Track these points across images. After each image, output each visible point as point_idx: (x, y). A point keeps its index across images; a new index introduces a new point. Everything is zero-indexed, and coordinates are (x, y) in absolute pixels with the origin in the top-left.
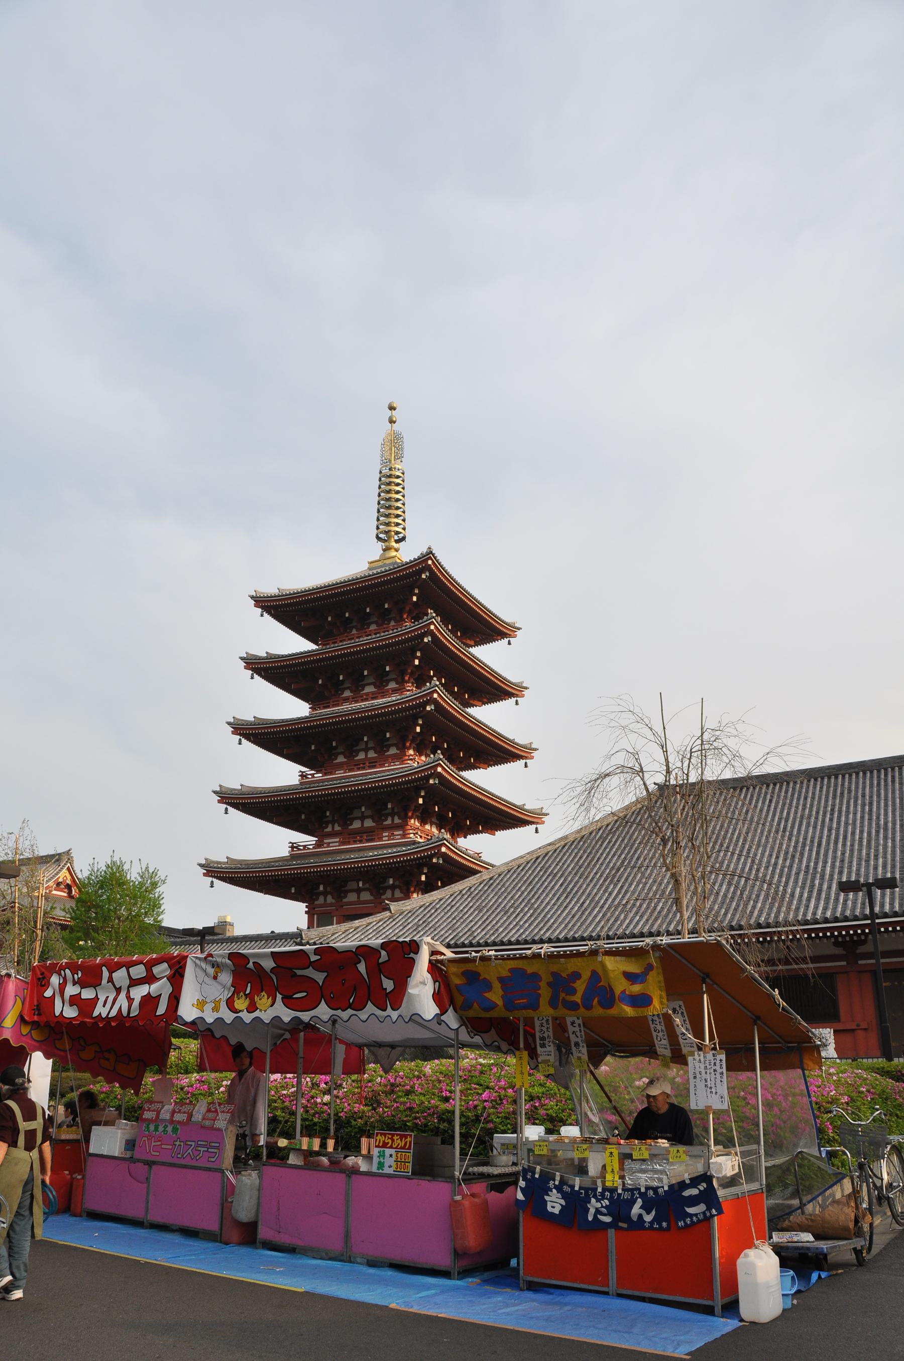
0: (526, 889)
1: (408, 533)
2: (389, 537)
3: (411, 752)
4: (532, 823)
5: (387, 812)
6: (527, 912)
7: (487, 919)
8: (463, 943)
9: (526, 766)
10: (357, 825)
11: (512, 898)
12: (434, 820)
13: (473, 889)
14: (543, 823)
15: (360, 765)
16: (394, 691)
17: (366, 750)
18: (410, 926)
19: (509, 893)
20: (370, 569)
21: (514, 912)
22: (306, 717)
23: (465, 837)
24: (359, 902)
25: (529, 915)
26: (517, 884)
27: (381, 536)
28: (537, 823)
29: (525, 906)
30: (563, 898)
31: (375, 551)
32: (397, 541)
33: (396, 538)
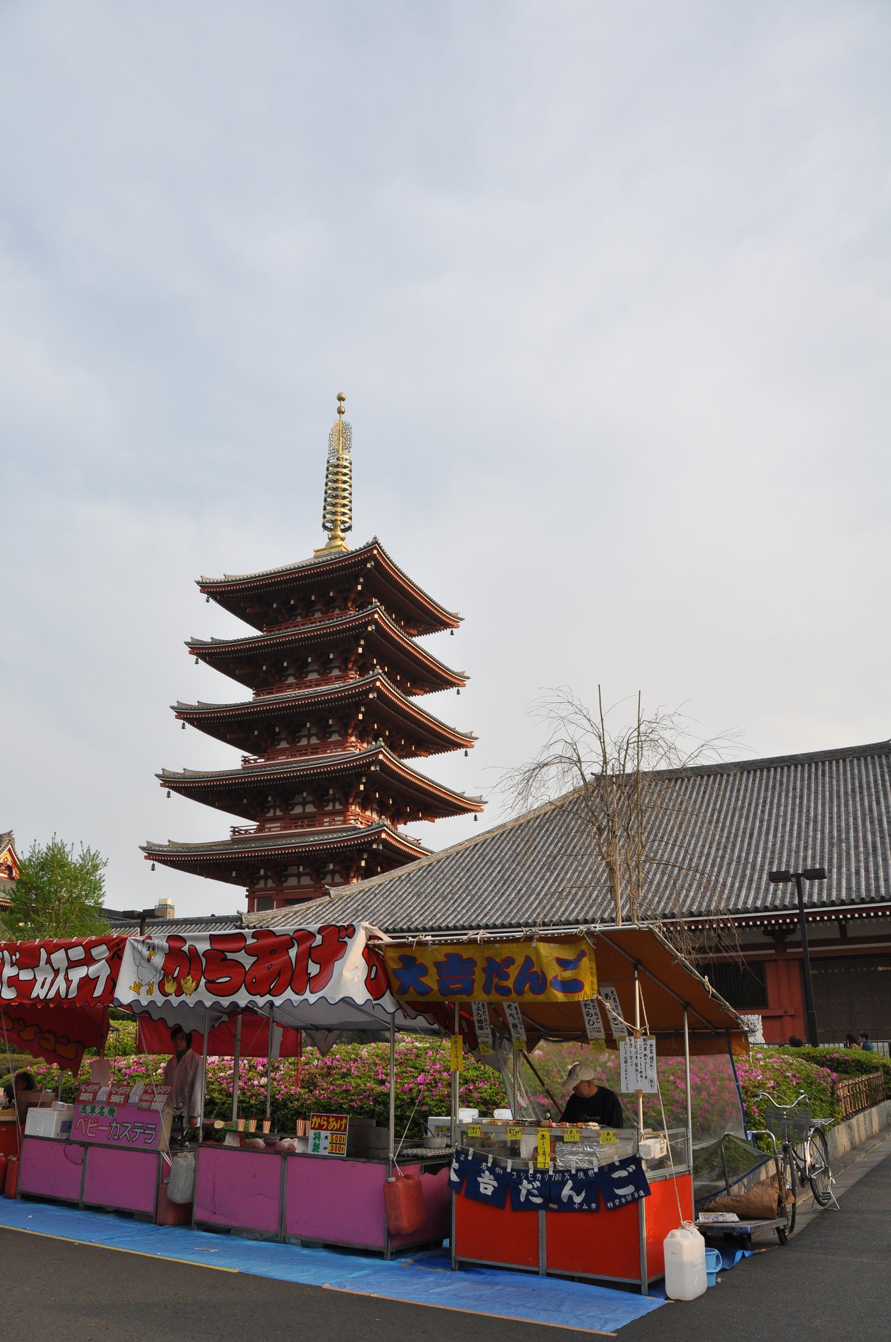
0: (464, 875)
1: (354, 523)
2: (336, 527)
3: (353, 739)
4: (472, 811)
5: (327, 798)
6: (465, 898)
7: (425, 904)
8: (401, 928)
9: (466, 754)
10: (298, 810)
11: (450, 884)
12: (375, 806)
13: (412, 875)
14: (482, 811)
15: (302, 751)
16: (338, 678)
17: (309, 736)
18: (349, 911)
19: (447, 880)
20: (316, 557)
21: (452, 898)
22: (250, 703)
23: (405, 824)
24: (299, 887)
26: (455, 871)
27: (328, 525)
28: (476, 811)
29: (463, 892)
30: (500, 885)
31: (321, 539)
32: (343, 531)
33: (342, 527)
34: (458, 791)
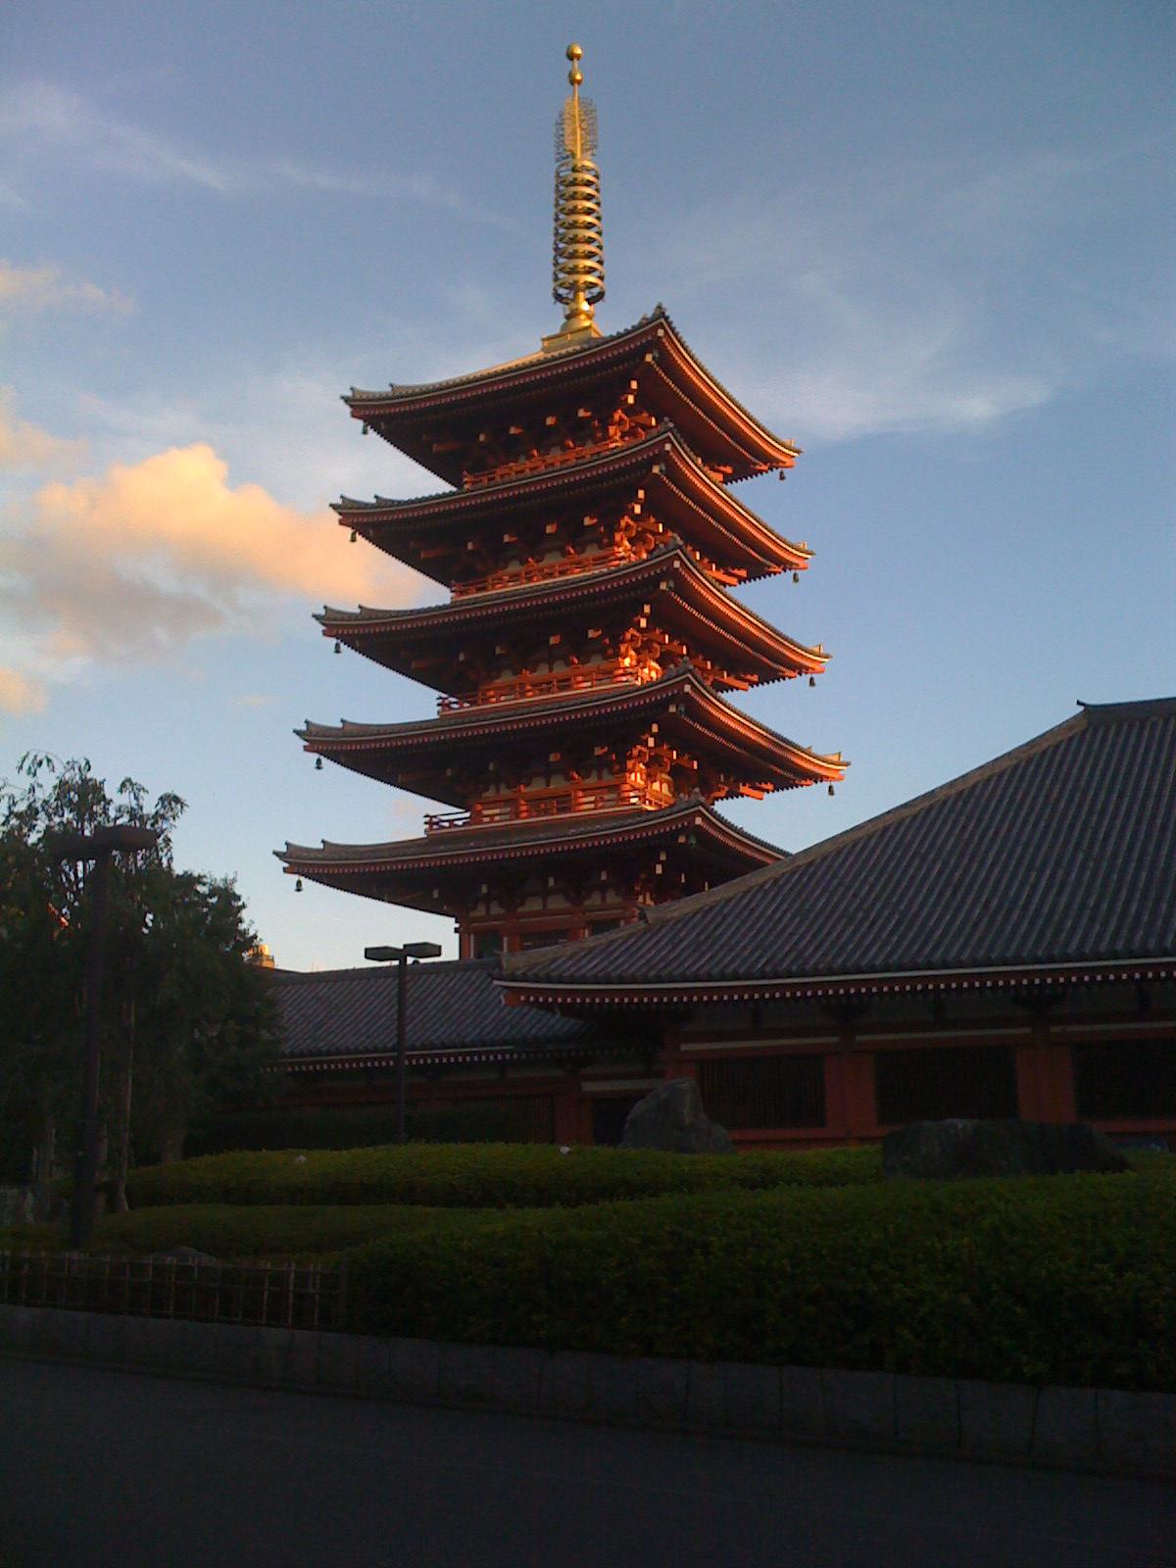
0: (877, 880)
13: (781, 883)
22: (445, 607)
26: (859, 873)
27: (562, 291)
30: (948, 894)
31: (553, 320)
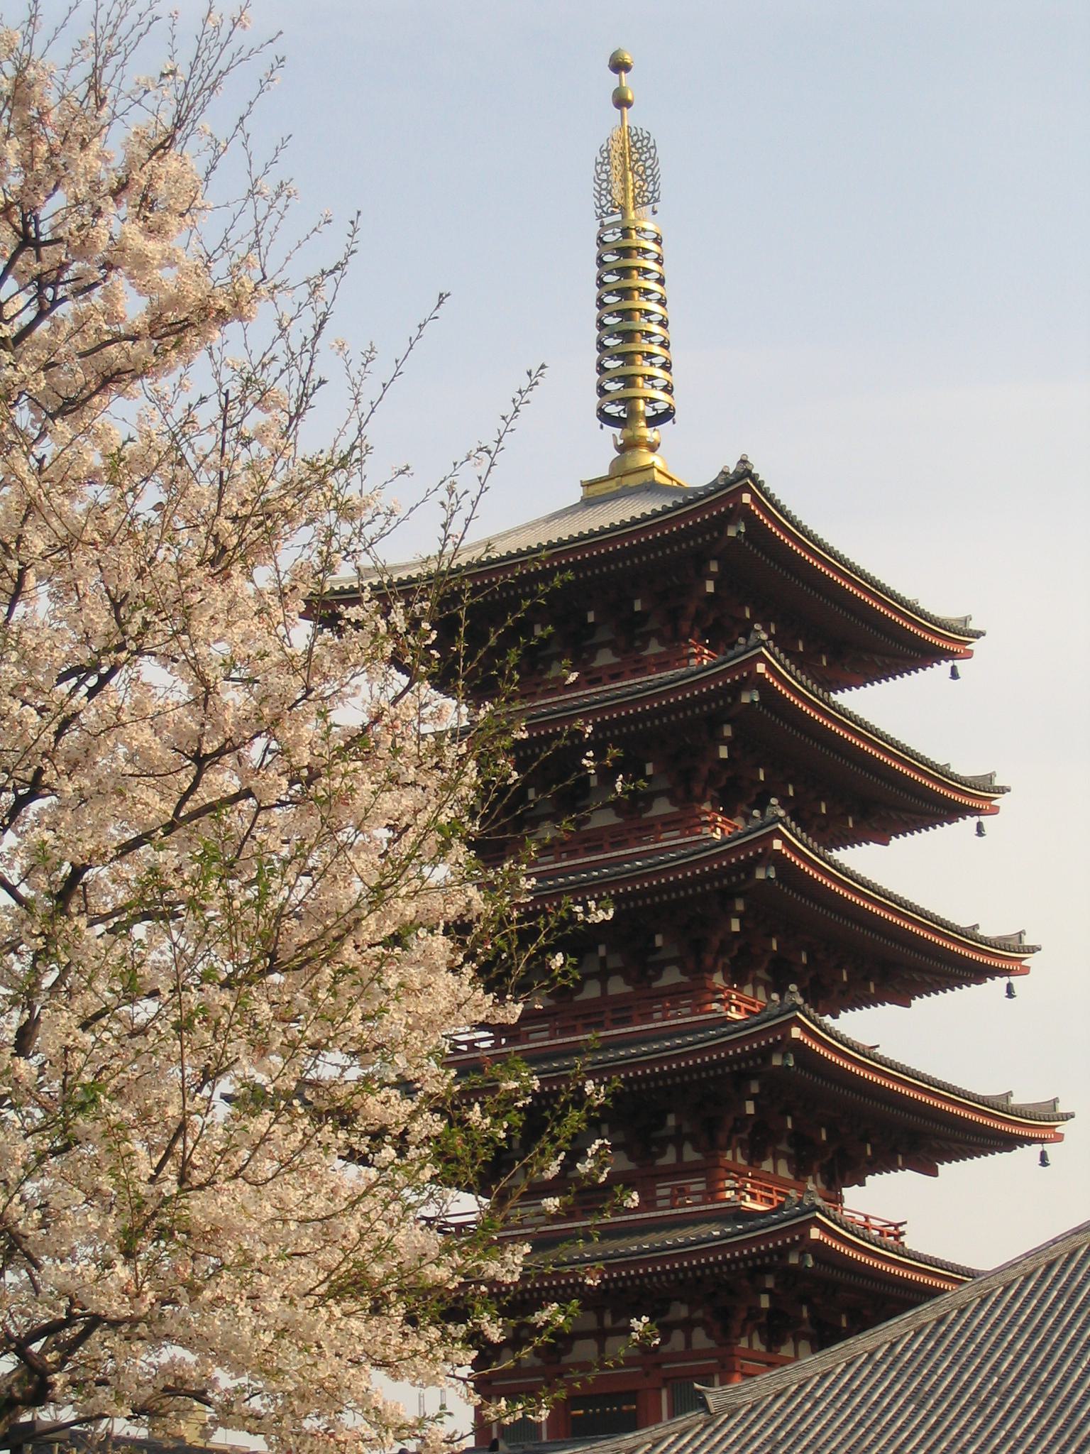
1: (678, 401)
3: (718, 980)
4: (1031, 1141)
5: (663, 1133)
6: (1031, 1405)
7: (938, 1423)
11: (994, 1369)
12: (783, 1147)
14: (1026, 971)
16: (668, 823)
19: (986, 1359)
21: (1000, 1405)
23: (862, 1184)
25: (1035, 1412)
27: (612, 410)
28: (1042, 1141)
29: (1027, 1390)
32: (653, 421)
34: (962, 920)
